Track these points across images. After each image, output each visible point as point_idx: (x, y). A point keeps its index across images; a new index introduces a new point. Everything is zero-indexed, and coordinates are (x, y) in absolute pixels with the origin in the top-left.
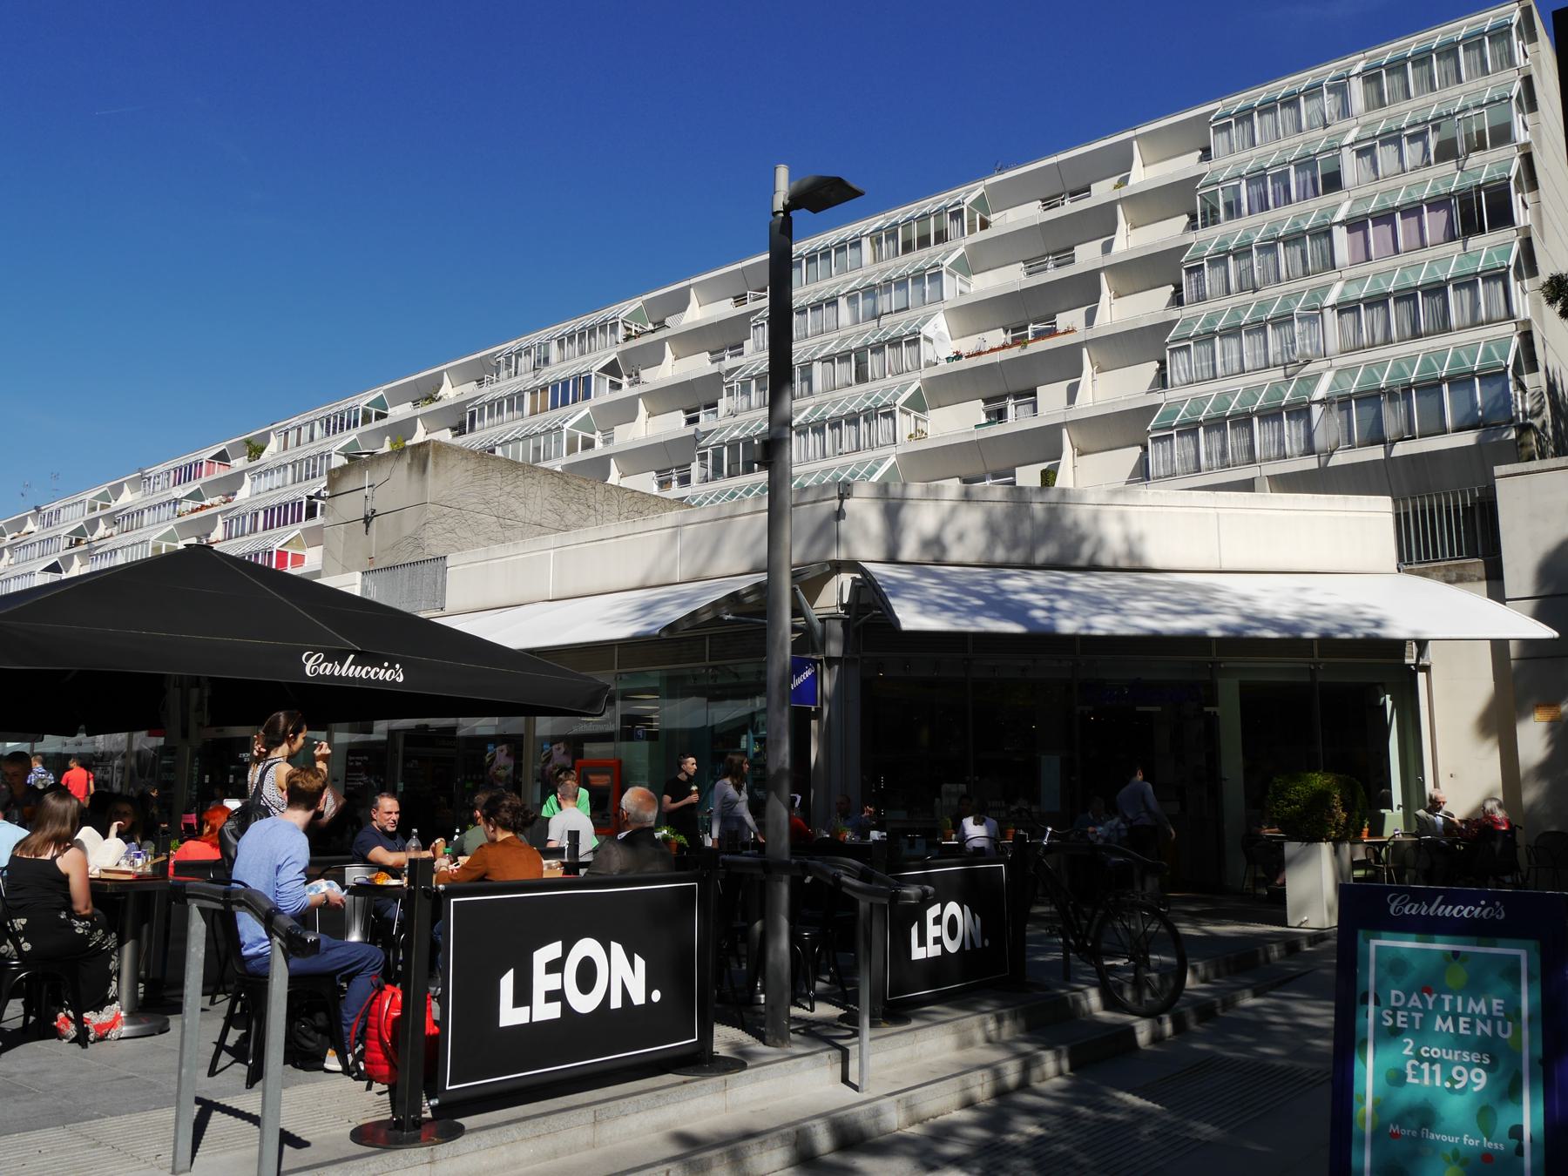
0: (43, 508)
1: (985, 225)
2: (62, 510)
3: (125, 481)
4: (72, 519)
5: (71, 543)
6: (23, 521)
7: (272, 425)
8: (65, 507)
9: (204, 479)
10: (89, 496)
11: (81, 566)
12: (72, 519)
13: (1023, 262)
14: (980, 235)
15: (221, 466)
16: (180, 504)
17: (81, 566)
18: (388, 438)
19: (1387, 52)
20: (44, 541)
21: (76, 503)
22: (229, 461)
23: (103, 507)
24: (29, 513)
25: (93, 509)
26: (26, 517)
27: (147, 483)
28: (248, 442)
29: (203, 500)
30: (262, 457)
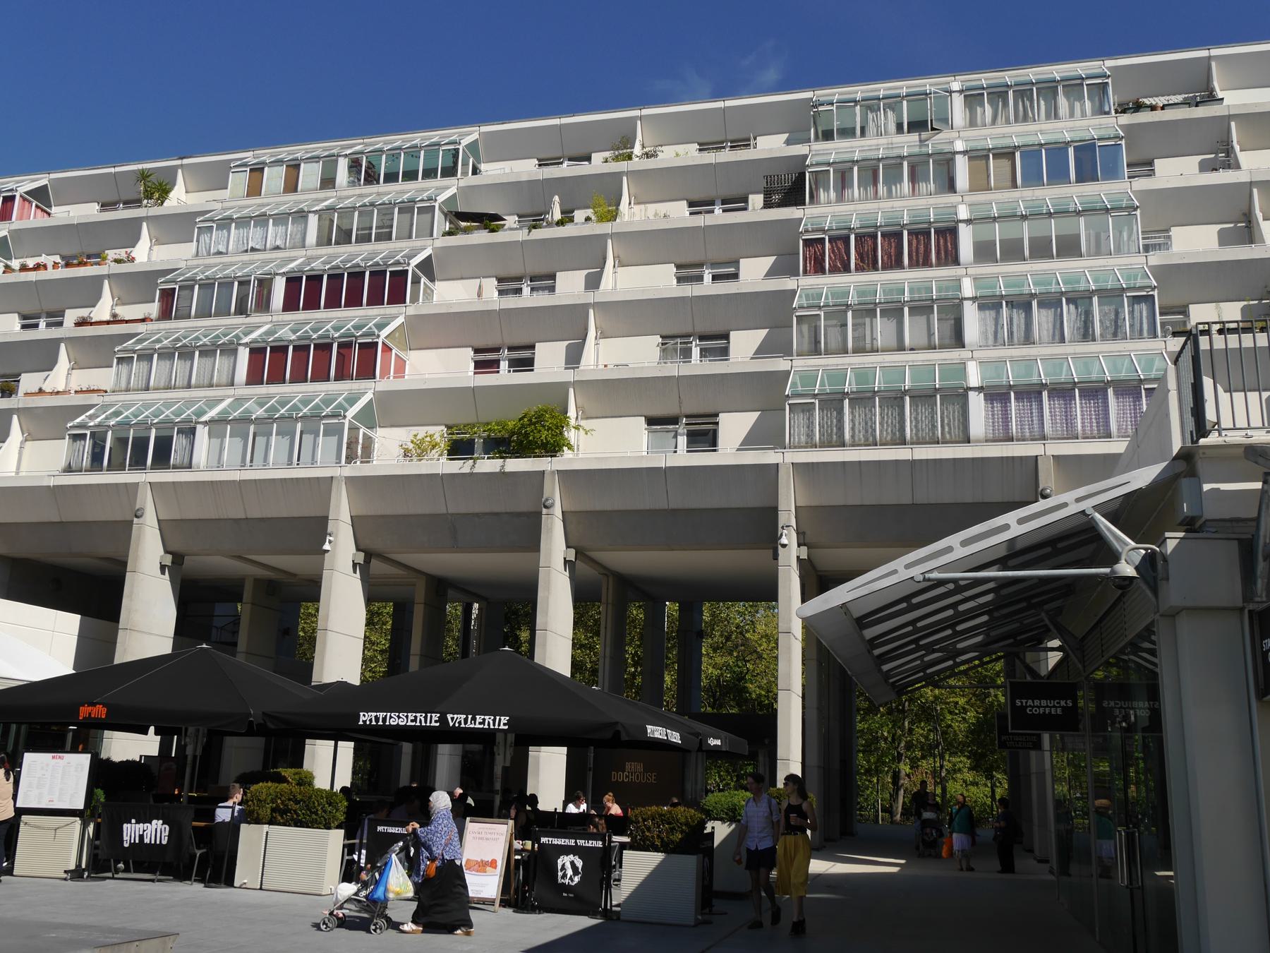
1: (475, 171)
7: (182, 158)
13: (518, 215)
14: (471, 180)
15: (39, 211)
18: (556, 198)
19: (985, 78)
22: (50, 207)
28: (144, 176)
29: (10, 259)
30: (165, 204)
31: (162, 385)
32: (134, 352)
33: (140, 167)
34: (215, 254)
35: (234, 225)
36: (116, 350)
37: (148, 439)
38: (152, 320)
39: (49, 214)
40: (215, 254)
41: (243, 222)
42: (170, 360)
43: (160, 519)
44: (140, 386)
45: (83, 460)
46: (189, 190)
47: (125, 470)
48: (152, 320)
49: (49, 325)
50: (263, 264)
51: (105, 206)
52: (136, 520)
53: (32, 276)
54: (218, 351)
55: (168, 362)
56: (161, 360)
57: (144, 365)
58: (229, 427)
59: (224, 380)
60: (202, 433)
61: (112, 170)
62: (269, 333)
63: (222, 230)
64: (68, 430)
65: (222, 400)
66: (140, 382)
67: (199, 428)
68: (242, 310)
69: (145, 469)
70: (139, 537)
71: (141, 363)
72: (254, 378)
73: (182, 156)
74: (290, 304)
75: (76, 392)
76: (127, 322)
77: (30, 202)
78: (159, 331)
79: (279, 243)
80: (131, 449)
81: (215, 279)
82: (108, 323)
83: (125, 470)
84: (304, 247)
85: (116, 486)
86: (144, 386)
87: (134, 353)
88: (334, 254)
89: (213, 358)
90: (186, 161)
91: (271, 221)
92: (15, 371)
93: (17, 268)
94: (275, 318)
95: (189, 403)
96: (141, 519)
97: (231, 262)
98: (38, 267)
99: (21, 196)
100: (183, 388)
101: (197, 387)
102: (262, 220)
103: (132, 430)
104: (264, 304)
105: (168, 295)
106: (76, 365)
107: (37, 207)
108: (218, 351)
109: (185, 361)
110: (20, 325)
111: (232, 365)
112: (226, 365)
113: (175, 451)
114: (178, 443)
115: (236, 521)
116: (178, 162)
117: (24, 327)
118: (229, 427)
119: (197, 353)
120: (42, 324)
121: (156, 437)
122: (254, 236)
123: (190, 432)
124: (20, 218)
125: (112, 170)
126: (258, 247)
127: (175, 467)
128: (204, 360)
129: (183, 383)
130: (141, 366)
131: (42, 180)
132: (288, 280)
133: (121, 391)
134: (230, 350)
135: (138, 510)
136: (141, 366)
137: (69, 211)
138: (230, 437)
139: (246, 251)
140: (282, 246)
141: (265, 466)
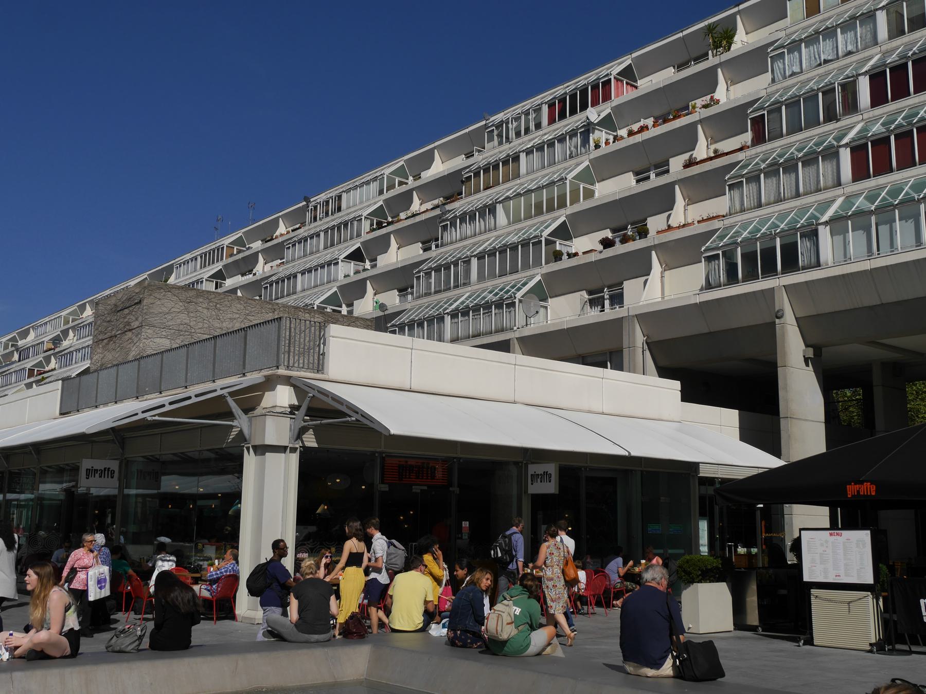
0: (312, 200)
2: (344, 196)
3: (435, 148)
4: (355, 205)
5: (372, 225)
6: (275, 224)
7: (738, 5)
8: (348, 191)
9: (616, 101)
10: (388, 170)
11: (399, 248)
12: (361, 202)
15: (629, 87)
16: (593, 133)
17: (399, 248)
20: (333, 228)
21: (368, 183)
22: (636, 81)
23: (401, 183)
24: (280, 214)
25: (391, 187)
26: (277, 220)
27: (496, 132)
28: (710, 29)
30: (732, 49)
31: (772, 199)
32: (742, 176)
33: (706, 23)
34: (791, 76)
35: (803, 44)
36: (726, 178)
37: (775, 248)
38: (748, 147)
39: (636, 87)
40: (791, 76)
41: (812, 40)
42: (775, 176)
43: (797, 317)
44: (752, 205)
45: (720, 277)
46: (748, 30)
47: (759, 279)
48: (748, 147)
49: (657, 175)
50: (840, 72)
51: (680, 67)
52: (777, 321)
53: (638, 138)
54: (820, 158)
55: (774, 179)
56: (768, 178)
57: (753, 186)
58: (850, 222)
59: (830, 183)
60: (824, 233)
61: (680, 35)
62: (864, 130)
63: (793, 53)
64: (702, 253)
65: (833, 201)
66: (752, 202)
67: (821, 229)
68: (831, 116)
69: (777, 275)
70: (783, 335)
71: (750, 185)
72: (860, 173)
73: (738, 3)
74: (878, 99)
75: (699, 222)
76: (727, 154)
77: (622, 81)
78: (757, 155)
79: (850, 48)
80: (761, 260)
81: (800, 96)
82: (711, 159)
83: (759, 279)
84: (877, 45)
85: (754, 293)
86: (756, 204)
87: (743, 177)
88: (910, 41)
89: (816, 166)
90: (742, 7)
91: (839, 30)
92: (641, 218)
93: (625, 135)
94: (866, 116)
95: (803, 210)
96: (782, 319)
97: (808, 79)
98: (643, 129)
99: (615, 78)
100: (792, 198)
101: (806, 194)
102: (829, 33)
103: (758, 243)
104: (851, 106)
105: (758, 122)
106: (691, 201)
107: (627, 83)
108: (820, 158)
109: (790, 174)
110: (635, 181)
111: (835, 167)
112: (830, 169)
113: (801, 254)
114: (803, 246)
115: (871, 308)
116: (736, 10)
117: (638, 181)
118: (850, 222)
119: (800, 164)
120: (653, 176)
121: (781, 246)
122: (825, 49)
123: (812, 235)
124: (617, 96)
125: (680, 35)
126: (830, 58)
127: (804, 268)
128: (806, 169)
129: (791, 194)
130: (751, 188)
131: (626, 61)
132: (871, 78)
133: (737, 213)
134: (832, 154)
135: (778, 311)
136: (751, 188)
137: (652, 80)
138: (852, 231)
139: (820, 65)
140: (855, 50)
141: (893, 251)
